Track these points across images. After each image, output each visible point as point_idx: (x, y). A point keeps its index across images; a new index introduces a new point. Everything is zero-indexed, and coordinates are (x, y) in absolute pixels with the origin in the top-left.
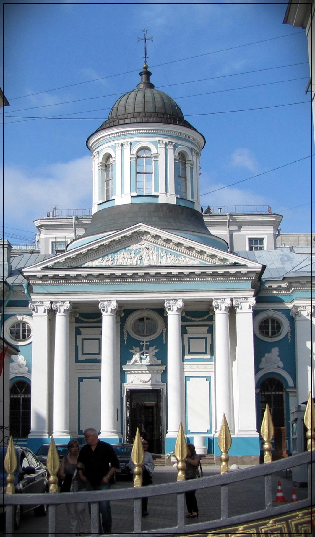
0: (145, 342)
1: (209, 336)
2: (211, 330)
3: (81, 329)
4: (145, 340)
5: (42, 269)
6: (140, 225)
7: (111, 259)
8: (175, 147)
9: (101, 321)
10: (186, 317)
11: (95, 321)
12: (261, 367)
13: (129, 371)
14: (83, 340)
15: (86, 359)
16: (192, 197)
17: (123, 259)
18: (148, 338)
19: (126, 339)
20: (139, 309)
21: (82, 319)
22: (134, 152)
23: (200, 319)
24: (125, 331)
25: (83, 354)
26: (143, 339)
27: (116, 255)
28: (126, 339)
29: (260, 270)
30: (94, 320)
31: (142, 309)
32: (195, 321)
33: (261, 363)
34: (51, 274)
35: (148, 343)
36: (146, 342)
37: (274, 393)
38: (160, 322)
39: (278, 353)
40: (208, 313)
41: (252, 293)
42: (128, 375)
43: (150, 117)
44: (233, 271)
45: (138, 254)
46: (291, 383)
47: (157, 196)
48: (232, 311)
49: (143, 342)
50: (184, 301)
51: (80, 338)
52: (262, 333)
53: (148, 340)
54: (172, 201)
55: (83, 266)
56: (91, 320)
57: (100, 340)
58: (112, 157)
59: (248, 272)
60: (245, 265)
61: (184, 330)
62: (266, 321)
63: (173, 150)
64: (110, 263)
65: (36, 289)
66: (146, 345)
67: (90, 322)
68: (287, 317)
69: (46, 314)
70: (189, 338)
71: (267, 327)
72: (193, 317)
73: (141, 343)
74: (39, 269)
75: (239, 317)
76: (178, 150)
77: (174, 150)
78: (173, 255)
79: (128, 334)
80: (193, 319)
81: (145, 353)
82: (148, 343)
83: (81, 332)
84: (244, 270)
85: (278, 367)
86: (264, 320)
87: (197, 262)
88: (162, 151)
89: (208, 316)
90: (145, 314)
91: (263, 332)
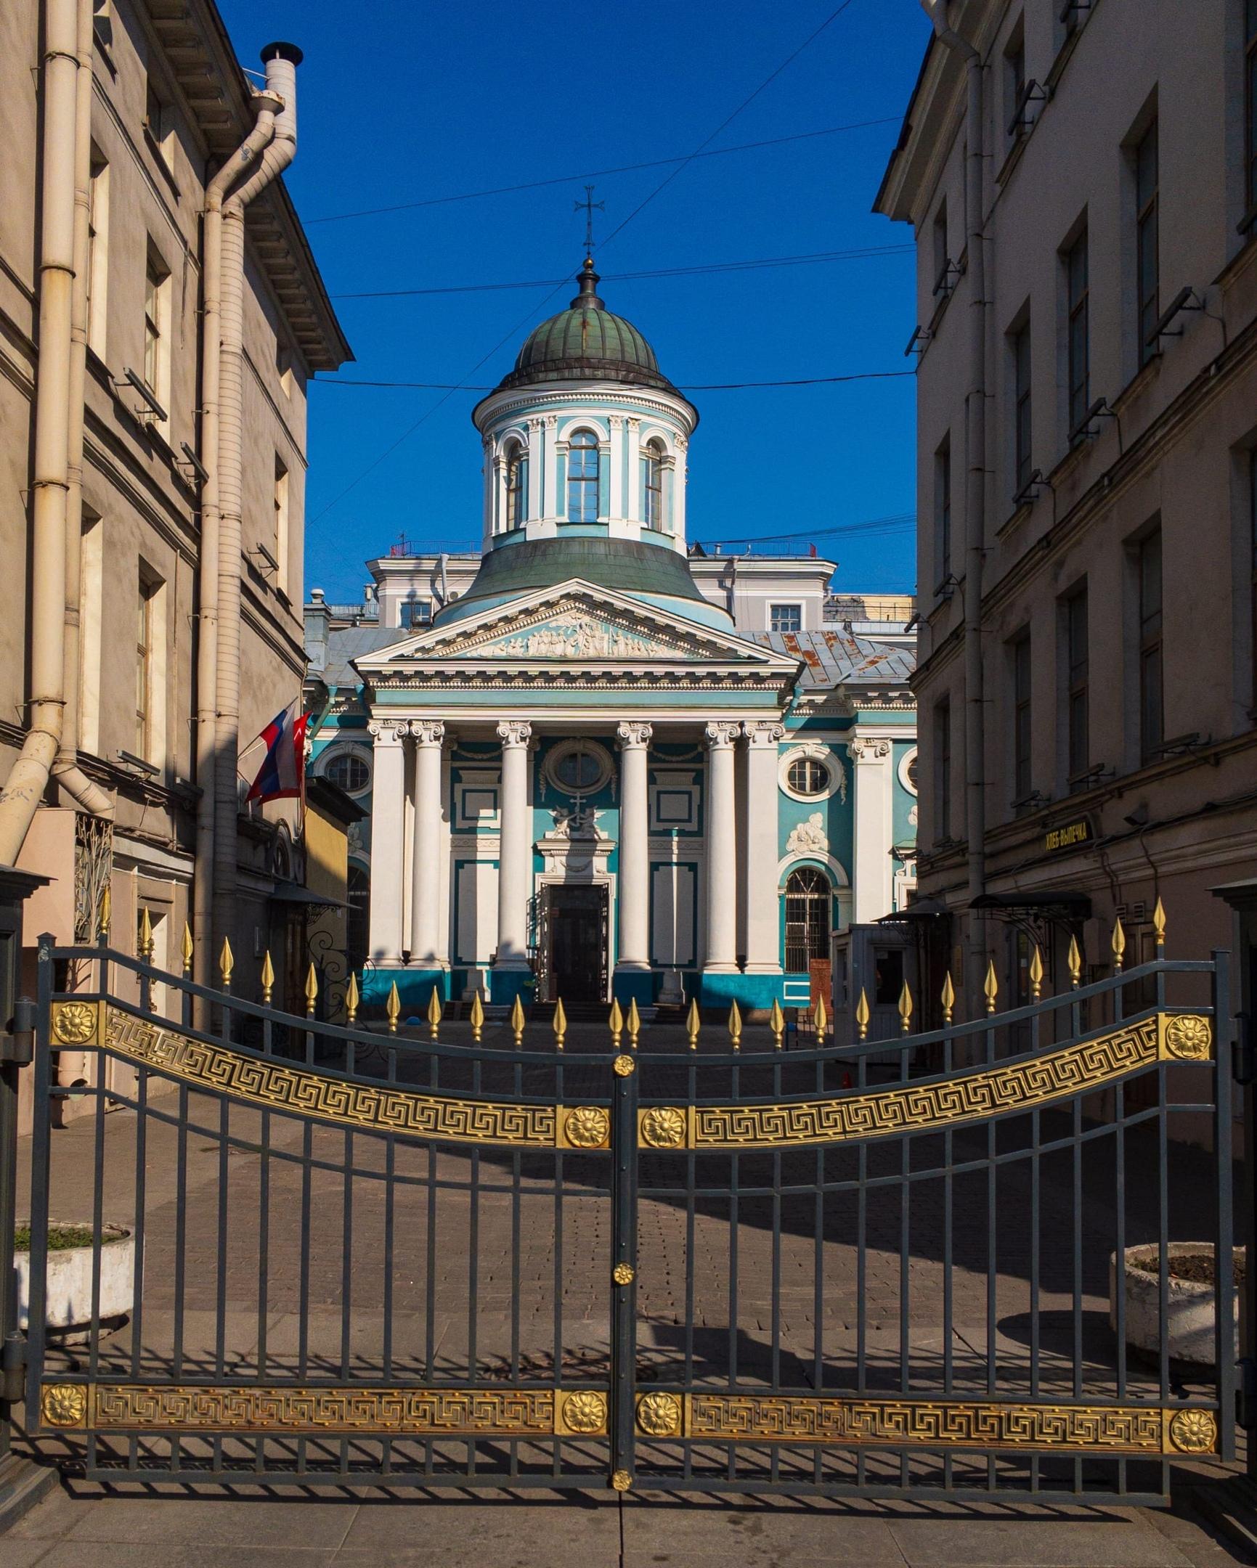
1: (696, 790)
2: (702, 778)
3: (461, 772)
4: (578, 795)
8: (644, 427)
9: (500, 758)
10: (655, 754)
12: (789, 848)
13: (550, 850)
14: (465, 791)
16: (671, 528)
17: (542, 645)
18: (583, 790)
19: (543, 791)
20: (568, 738)
22: (565, 436)
23: (681, 758)
24: (541, 777)
27: (530, 637)
28: (543, 791)
29: (795, 671)
30: (485, 757)
31: (574, 738)
32: (672, 762)
33: (791, 840)
34: (409, 669)
35: (584, 801)
36: (581, 798)
38: (607, 762)
39: (820, 825)
40: (694, 747)
41: (777, 714)
42: (547, 858)
43: (597, 368)
44: (744, 671)
45: (572, 635)
46: (842, 877)
47: (607, 524)
48: (741, 744)
49: (575, 798)
50: (654, 725)
51: (459, 788)
52: (793, 787)
54: (634, 534)
55: (469, 655)
57: (495, 792)
58: (521, 445)
59: (773, 674)
60: (767, 661)
61: (651, 780)
62: (801, 762)
63: (637, 435)
64: (519, 652)
65: (381, 696)
67: (479, 760)
68: (839, 758)
69: (399, 742)
70: (659, 793)
71: (802, 776)
72: (666, 753)
73: (572, 801)
74: (386, 659)
75: (754, 757)
76: (649, 435)
77: (640, 435)
78: (636, 641)
79: (548, 783)
80: (668, 758)
82: (584, 801)
83: (460, 777)
84: (764, 671)
85: (820, 849)
87: (678, 655)
88: (617, 435)
89: (696, 752)
90: (578, 747)
91: (794, 785)
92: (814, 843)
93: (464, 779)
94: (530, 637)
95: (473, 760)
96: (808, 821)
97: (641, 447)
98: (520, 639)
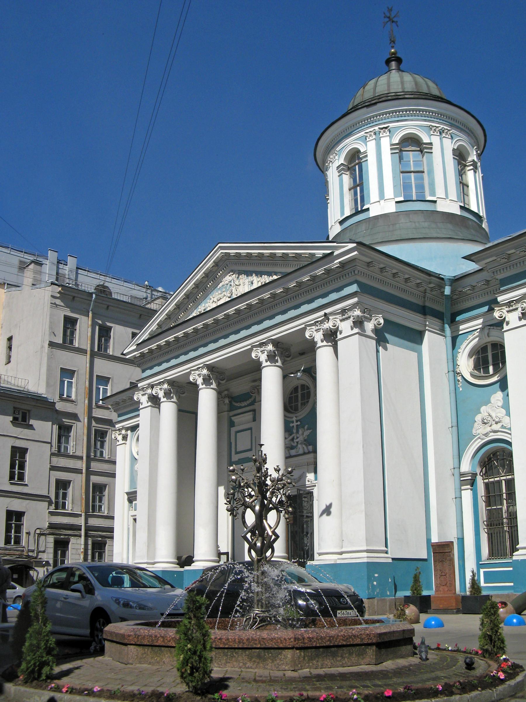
0: (295, 422)
3: (233, 418)
5: (138, 345)
6: (220, 247)
7: (203, 308)
11: (251, 401)
15: (239, 459)
16: (433, 194)
21: (236, 404)
25: (237, 453)
26: (292, 418)
33: (476, 425)
35: (299, 423)
36: (297, 421)
37: (504, 478)
49: (293, 422)
51: (233, 430)
53: (298, 418)
56: (245, 404)
66: (297, 425)
73: (291, 425)
81: (295, 438)
82: (299, 423)
86: (480, 349)
92: (497, 423)
93: (236, 424)
94: (208, 301)
95: (241, 407)
96: (489, 402)
97: (392, 145)
98: (203, 305)
